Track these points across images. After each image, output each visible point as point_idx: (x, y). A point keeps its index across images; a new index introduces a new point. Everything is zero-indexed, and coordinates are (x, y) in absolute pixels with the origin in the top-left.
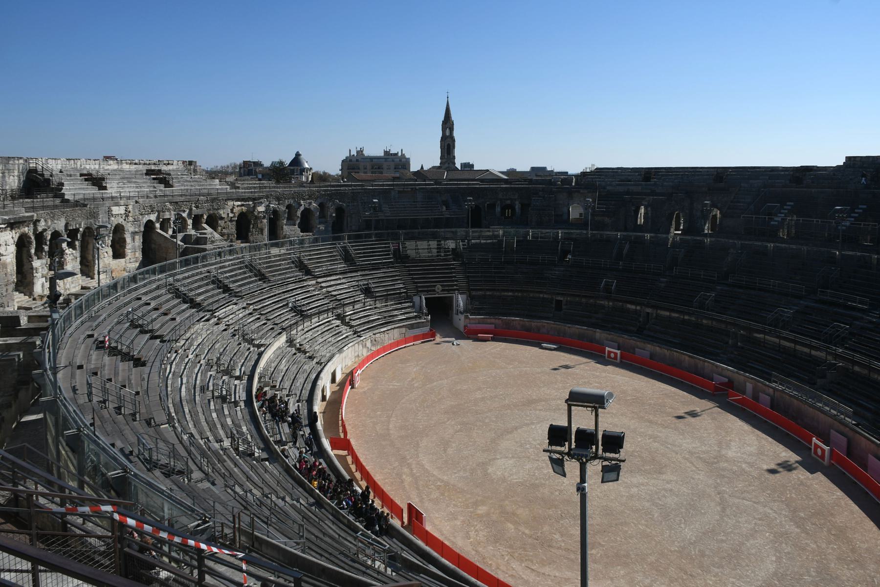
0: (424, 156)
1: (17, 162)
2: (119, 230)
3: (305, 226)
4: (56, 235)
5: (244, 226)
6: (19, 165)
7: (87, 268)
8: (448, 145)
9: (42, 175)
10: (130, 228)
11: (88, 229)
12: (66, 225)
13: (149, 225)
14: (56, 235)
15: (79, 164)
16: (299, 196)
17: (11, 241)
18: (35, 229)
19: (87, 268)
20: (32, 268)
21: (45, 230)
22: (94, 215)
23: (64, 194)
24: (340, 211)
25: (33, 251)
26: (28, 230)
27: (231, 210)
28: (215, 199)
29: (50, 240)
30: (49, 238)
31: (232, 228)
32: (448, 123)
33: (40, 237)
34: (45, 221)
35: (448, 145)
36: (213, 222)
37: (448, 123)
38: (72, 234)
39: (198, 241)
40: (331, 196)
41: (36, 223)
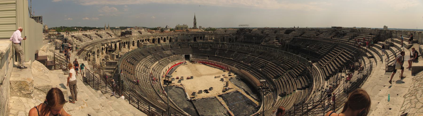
0: (191, 25)
2: (133, 42)
3: (165, 41)
4: (124, 43)
5: (154, 41)
7: (129, 47)
8: (195, 24)
10: (135, 41)
13: (138, 41)
14: (124, 43)
16: (163, 36)
19: (129, 47)
22: (130, 39)
24: (171, 38)
27: (151, 38)
28: (149, 36)
31: (152, 41)
32: (195, 19)
35: (195, 24)
36: (148, 40)
37: (195, 19)
39: (146, 44)
40: (169, 35)
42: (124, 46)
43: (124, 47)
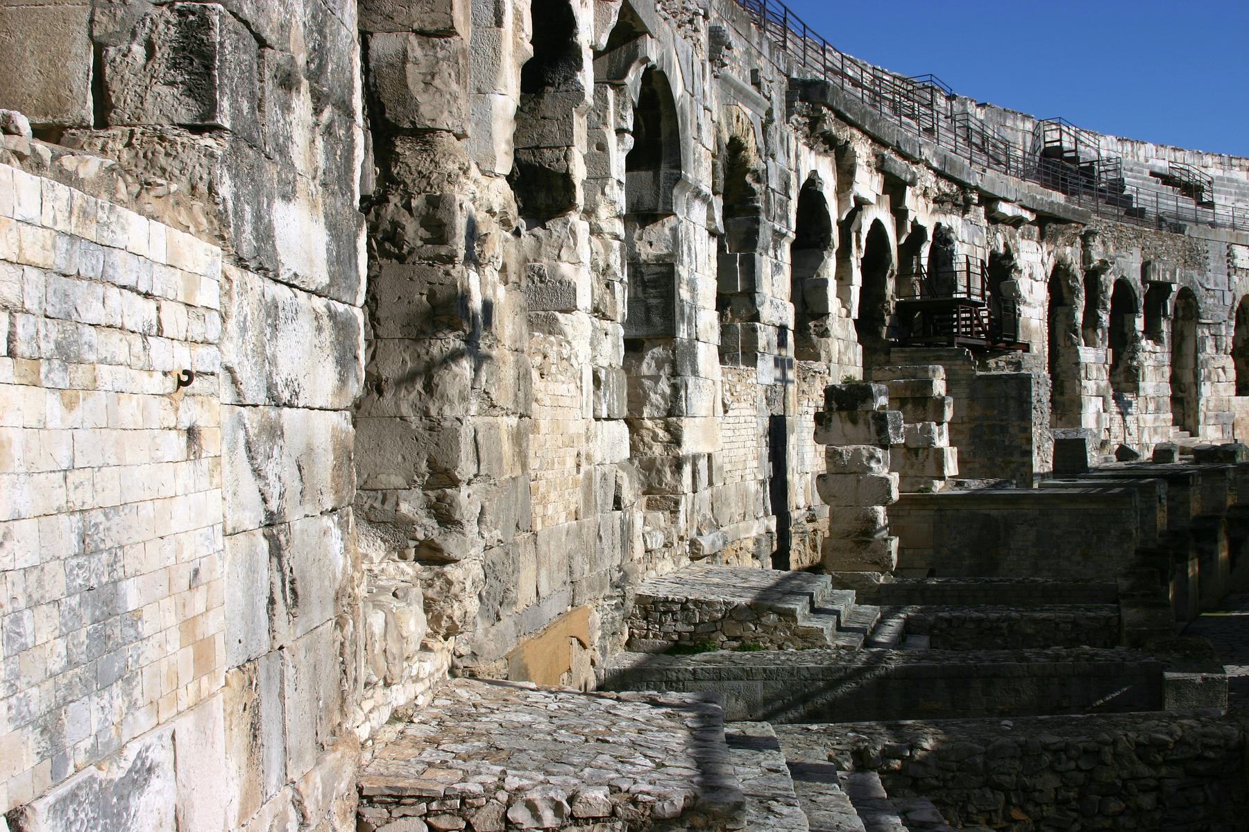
1: (1020, 125)
4: (1122, 285)
6: (1024, 132)
9: (1075, 160)
11: (1186, 295)
12: (1145, 267)
14: (1122, 285)
15: (1141, 153)
17: (1040, 272)
18: (1086, 258)
20: (1078, 364)
21: (1104, 266)
23: (1130, 197)
25: (1079, 316)
26: (1072, 254)
29: (1113, 299)
30: (1111, 292)
33: (1092, 277)
34: (1104, 243)
38: (1159, 291)
41: (1086, 238)
42: (1122, 343)
43: (1124, 379)
